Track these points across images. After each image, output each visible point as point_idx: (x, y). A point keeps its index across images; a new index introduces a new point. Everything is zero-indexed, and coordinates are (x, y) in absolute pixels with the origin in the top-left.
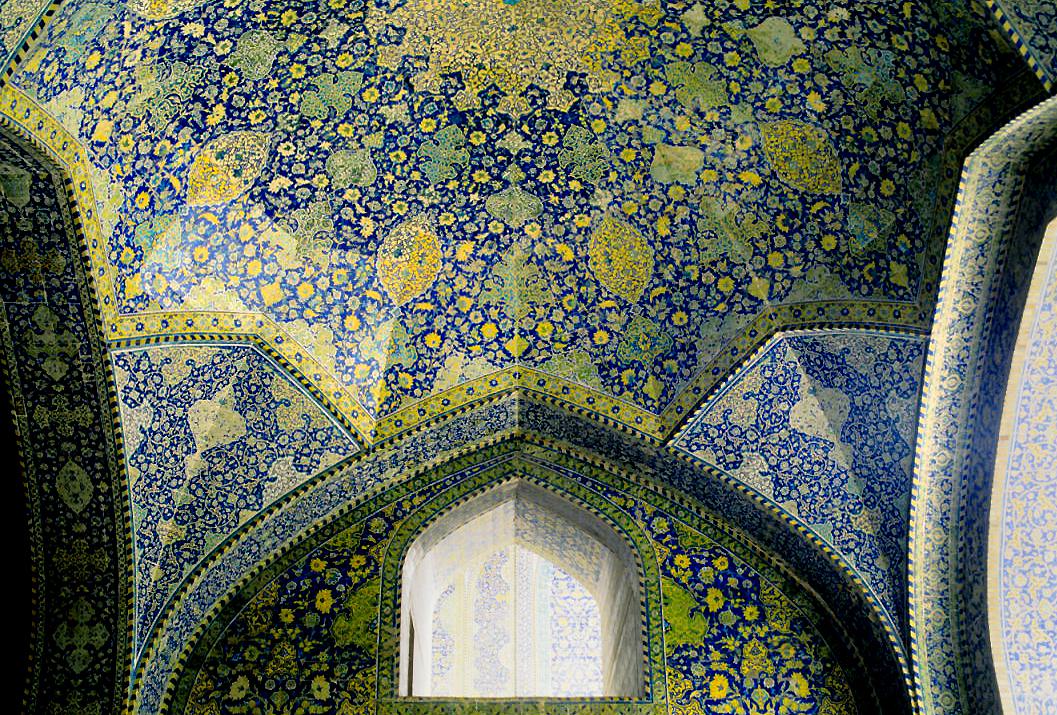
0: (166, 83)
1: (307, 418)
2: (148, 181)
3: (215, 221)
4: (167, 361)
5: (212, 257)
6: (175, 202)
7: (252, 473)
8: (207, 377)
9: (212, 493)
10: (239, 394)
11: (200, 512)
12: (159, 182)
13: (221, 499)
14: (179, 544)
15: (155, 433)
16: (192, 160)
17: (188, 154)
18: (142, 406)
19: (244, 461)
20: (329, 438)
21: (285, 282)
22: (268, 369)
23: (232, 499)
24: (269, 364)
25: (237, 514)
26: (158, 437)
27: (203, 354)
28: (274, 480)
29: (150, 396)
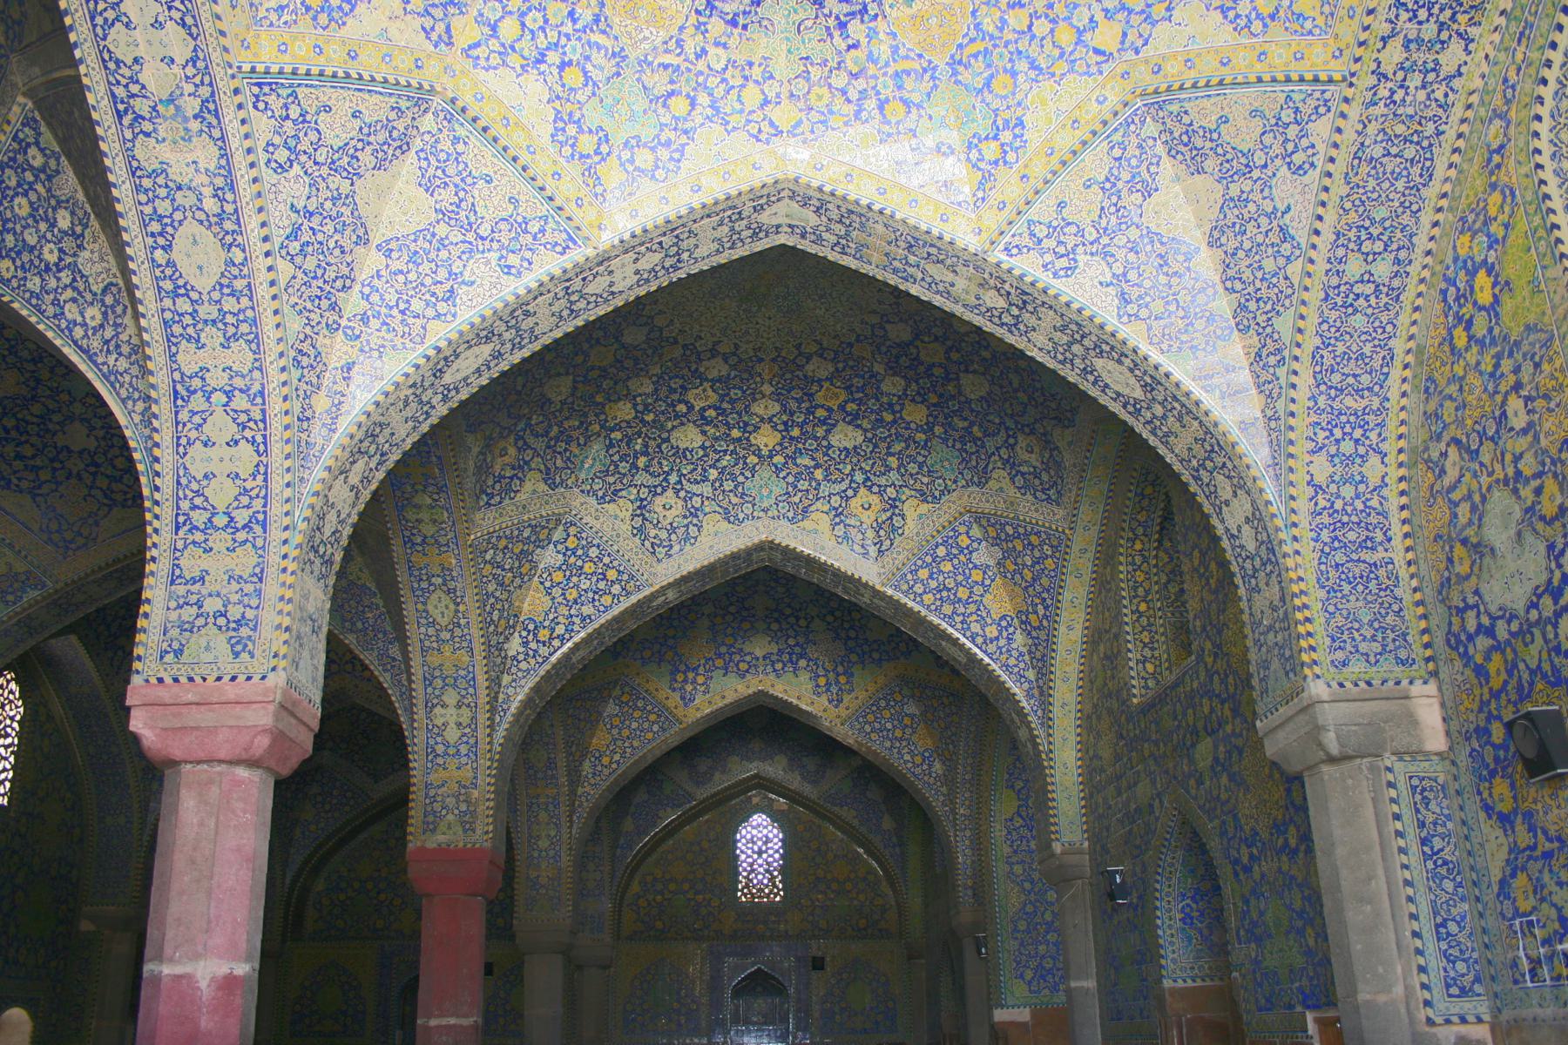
0: (778, 28)
1: (1254, 113)
2: (878, 93)
3: (979, 46)
4: (1061, 205)
5: (1014, 74)
6: (927, 76)
7: (1264, 221)
8: (1125, 176)
9: (1247, 275)
10: (1179, 157)
11: (1252, 305)
12: (890, 83)
13: (1259, 275)
14: (1258, 355)
15: (1125, 275)
16: (894, 35)
17: (882, 36)
18: (1081, 264)
19: (1246, 216)
20: (1297, 110)
21: (1106, 11)
22: (1175, 108)
23: (1269, 265)
24: (1171, 102)
25: (1286, 278)
26: (1132, 275)
27: (1096, 162)
28: (1289, 208)
29: (1080, 249)
